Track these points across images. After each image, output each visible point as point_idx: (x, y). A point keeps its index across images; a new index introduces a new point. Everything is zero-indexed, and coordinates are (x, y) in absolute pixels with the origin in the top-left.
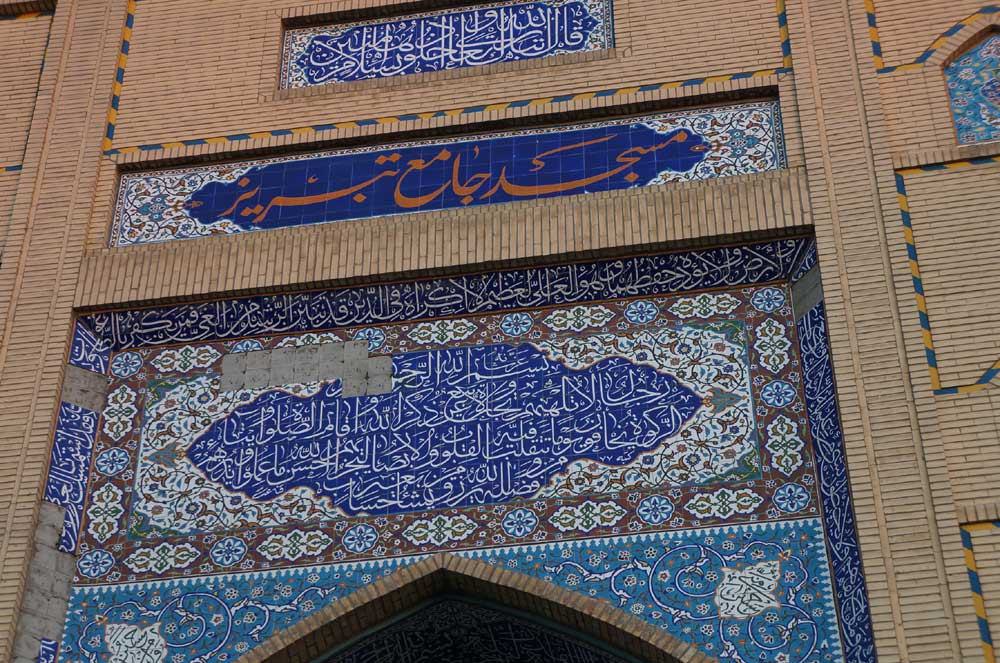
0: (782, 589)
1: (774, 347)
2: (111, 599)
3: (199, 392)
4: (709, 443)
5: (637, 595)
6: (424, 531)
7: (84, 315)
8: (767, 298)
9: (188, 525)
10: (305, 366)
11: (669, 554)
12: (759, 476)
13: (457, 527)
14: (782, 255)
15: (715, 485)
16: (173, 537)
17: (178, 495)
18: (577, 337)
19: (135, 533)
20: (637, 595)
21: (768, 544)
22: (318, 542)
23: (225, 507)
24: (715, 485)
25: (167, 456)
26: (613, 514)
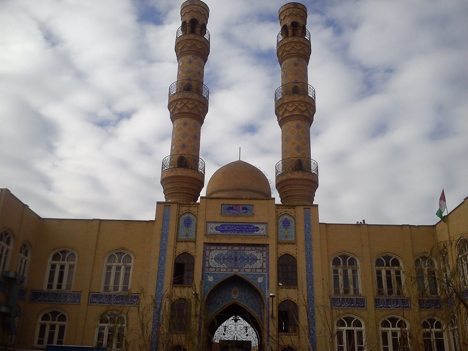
0: (263, 280)
1: (265, 253)
2: (208, 273)
3: (214, 253)
4: (258, 264)
5: (252, 279)
6: (234, 270)
7: (204, 243)
8: (265, 249)
9: (214, 266)
10: (224, 251)
11: (254, 275)
12: (262, 268)
13: (237, 270)
14: (266, 245)
15: (258, 269)
16: (213, 268)
17: (213, 263)
18: (248, 252)
19: (210, 267)
20: (252, 279)
21: (262, 275)
22: (225, 270)
23: (218, 265)
24: (258, 269)
25: (212, 259)
26: (249, 270)
